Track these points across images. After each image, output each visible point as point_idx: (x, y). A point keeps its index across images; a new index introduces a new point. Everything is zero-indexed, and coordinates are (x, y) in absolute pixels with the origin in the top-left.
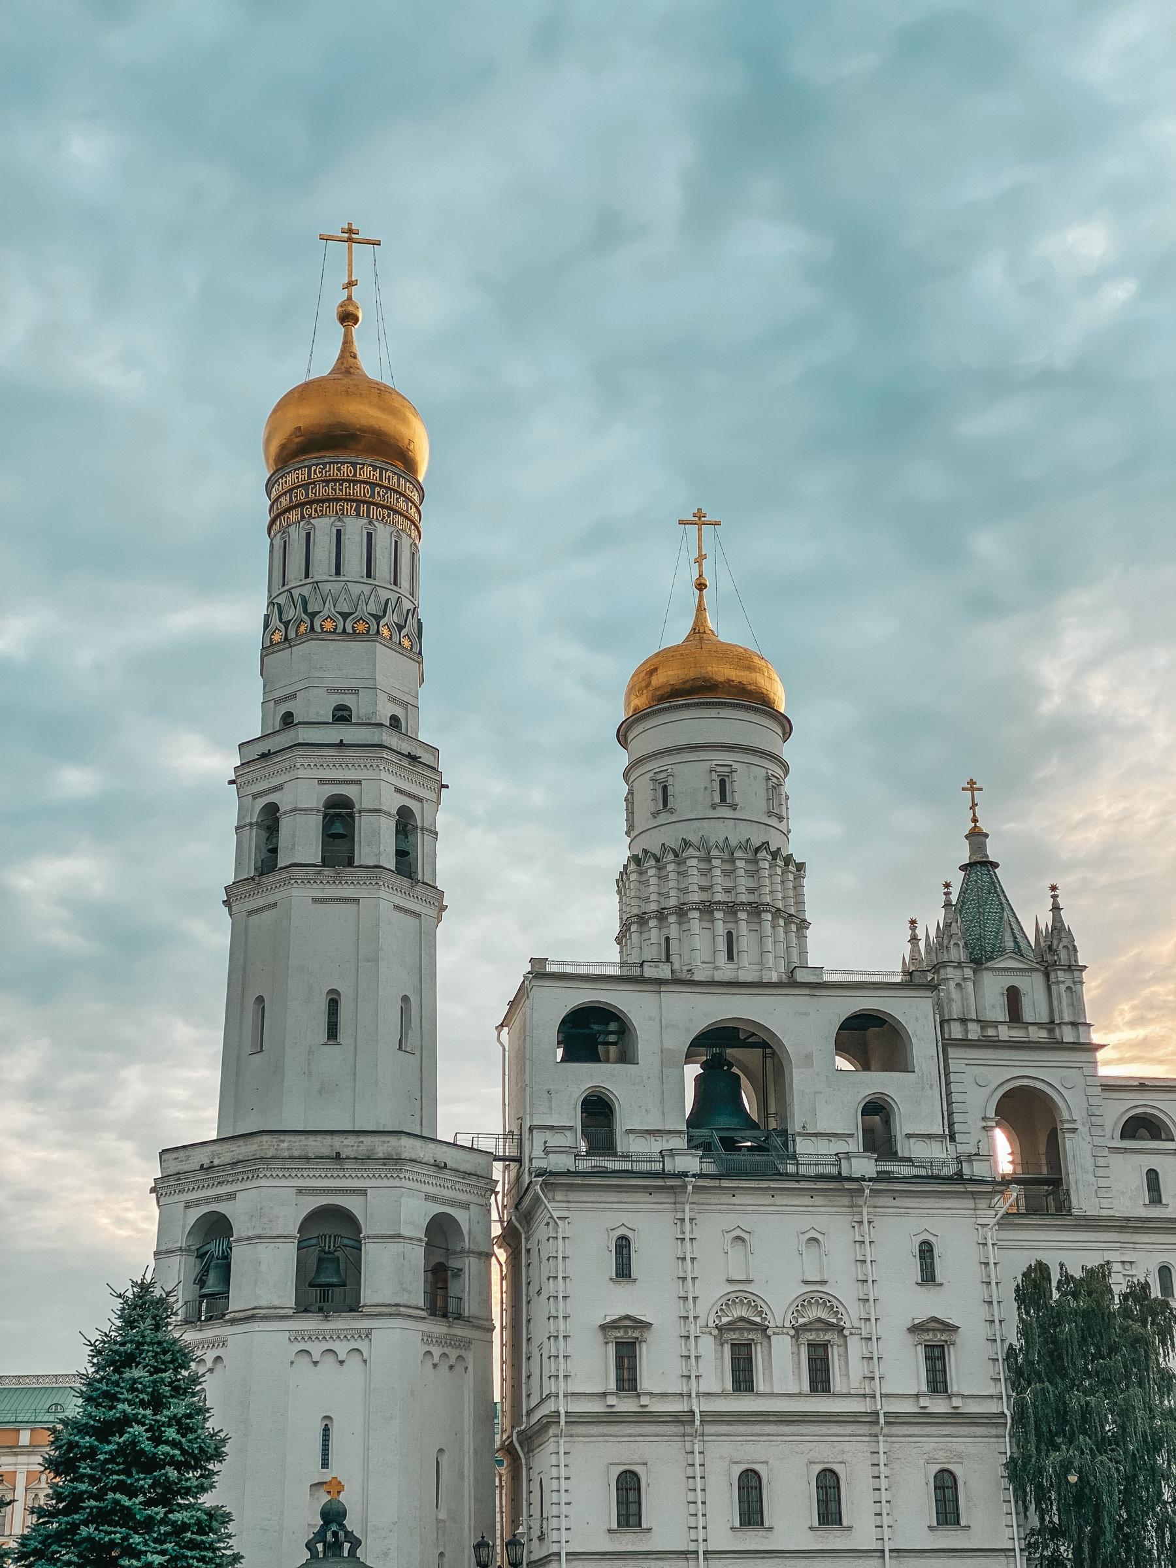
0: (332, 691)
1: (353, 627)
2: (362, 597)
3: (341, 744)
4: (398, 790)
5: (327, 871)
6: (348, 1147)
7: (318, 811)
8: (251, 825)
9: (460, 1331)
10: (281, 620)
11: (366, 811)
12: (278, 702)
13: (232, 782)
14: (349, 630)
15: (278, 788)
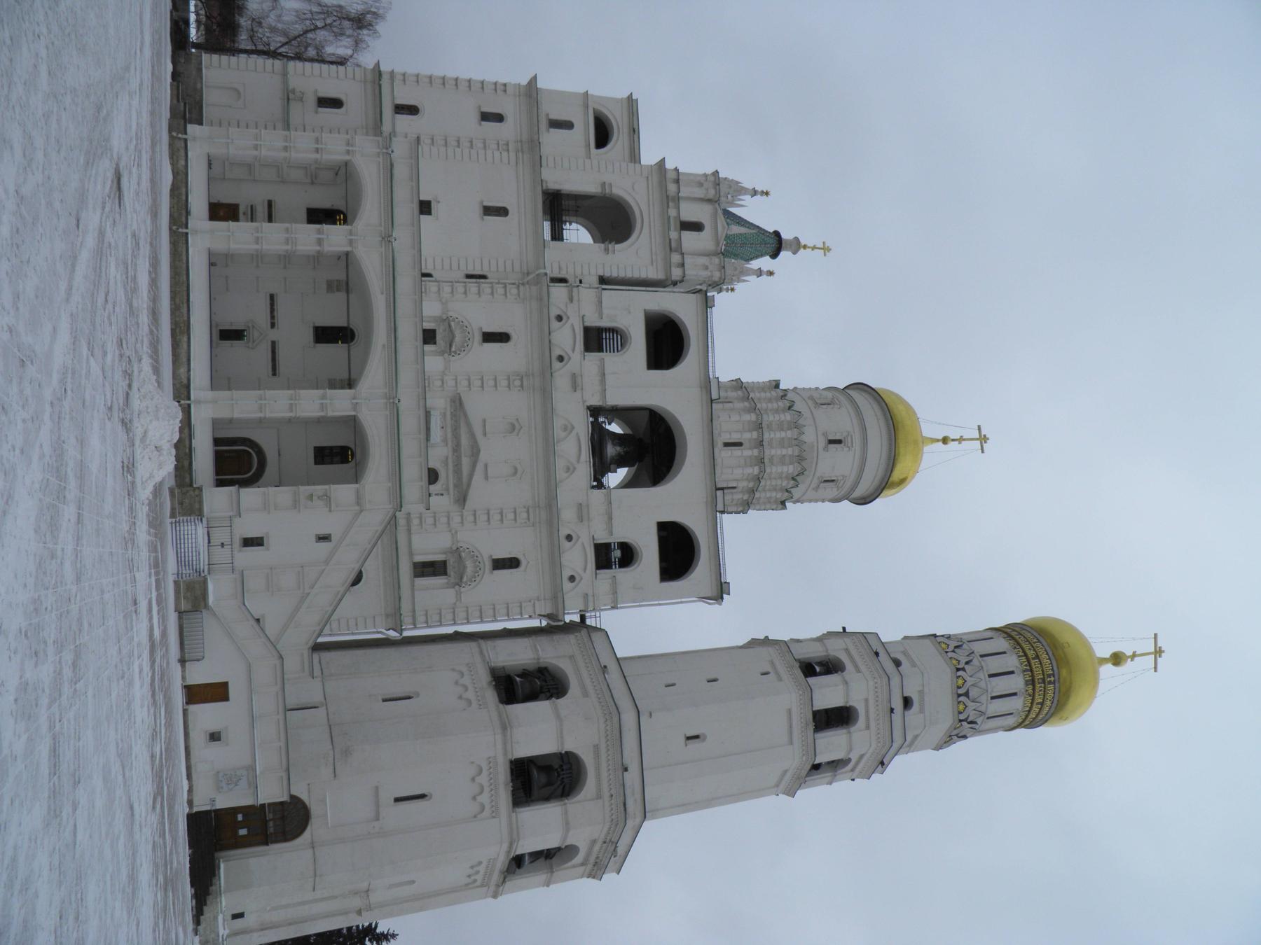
0: (921, 693)
1: (960, 702)
2: (978, 704)
3: (892, 710)
4: (862, 757)
5: (810, 716)
6: (632, 777)
7: (847, 702)
8: (827, 651)
9: (496, 877)
10: (956, 647)
11: (850, 737)
12: (905, 653)
13: (844, 628)
14: (962, 699)
15: (858, 671)
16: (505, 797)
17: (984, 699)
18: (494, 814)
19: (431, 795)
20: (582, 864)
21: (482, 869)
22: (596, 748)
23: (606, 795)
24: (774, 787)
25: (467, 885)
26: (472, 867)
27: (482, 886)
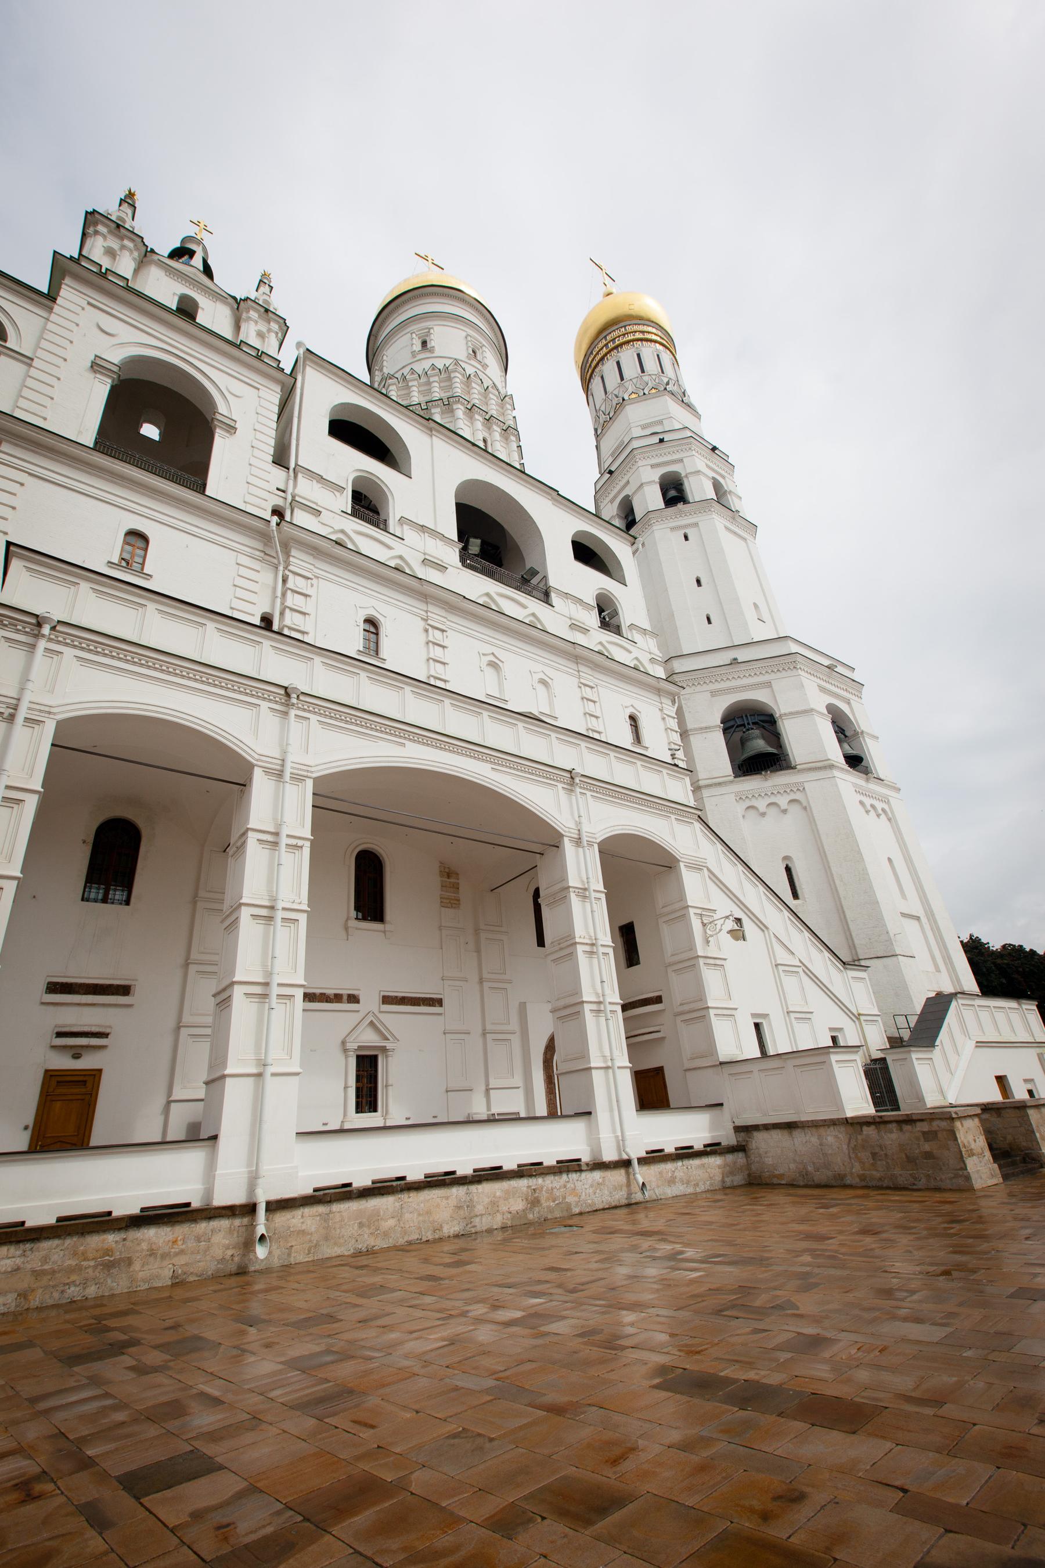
0: (644, 427)
5: (672, 510)
9: (873, 786)
14: (646, 393)
16: (779, 779)
17: (646, 378)
18: (801, 789)
19: (786, 858)
20: (848, 702)
21: (868, 802)
22: (714, 693)
23: (766, 678)
24: (746, 543)
25: (889, 820)
26: (867, 812)
27: (888, 803)
